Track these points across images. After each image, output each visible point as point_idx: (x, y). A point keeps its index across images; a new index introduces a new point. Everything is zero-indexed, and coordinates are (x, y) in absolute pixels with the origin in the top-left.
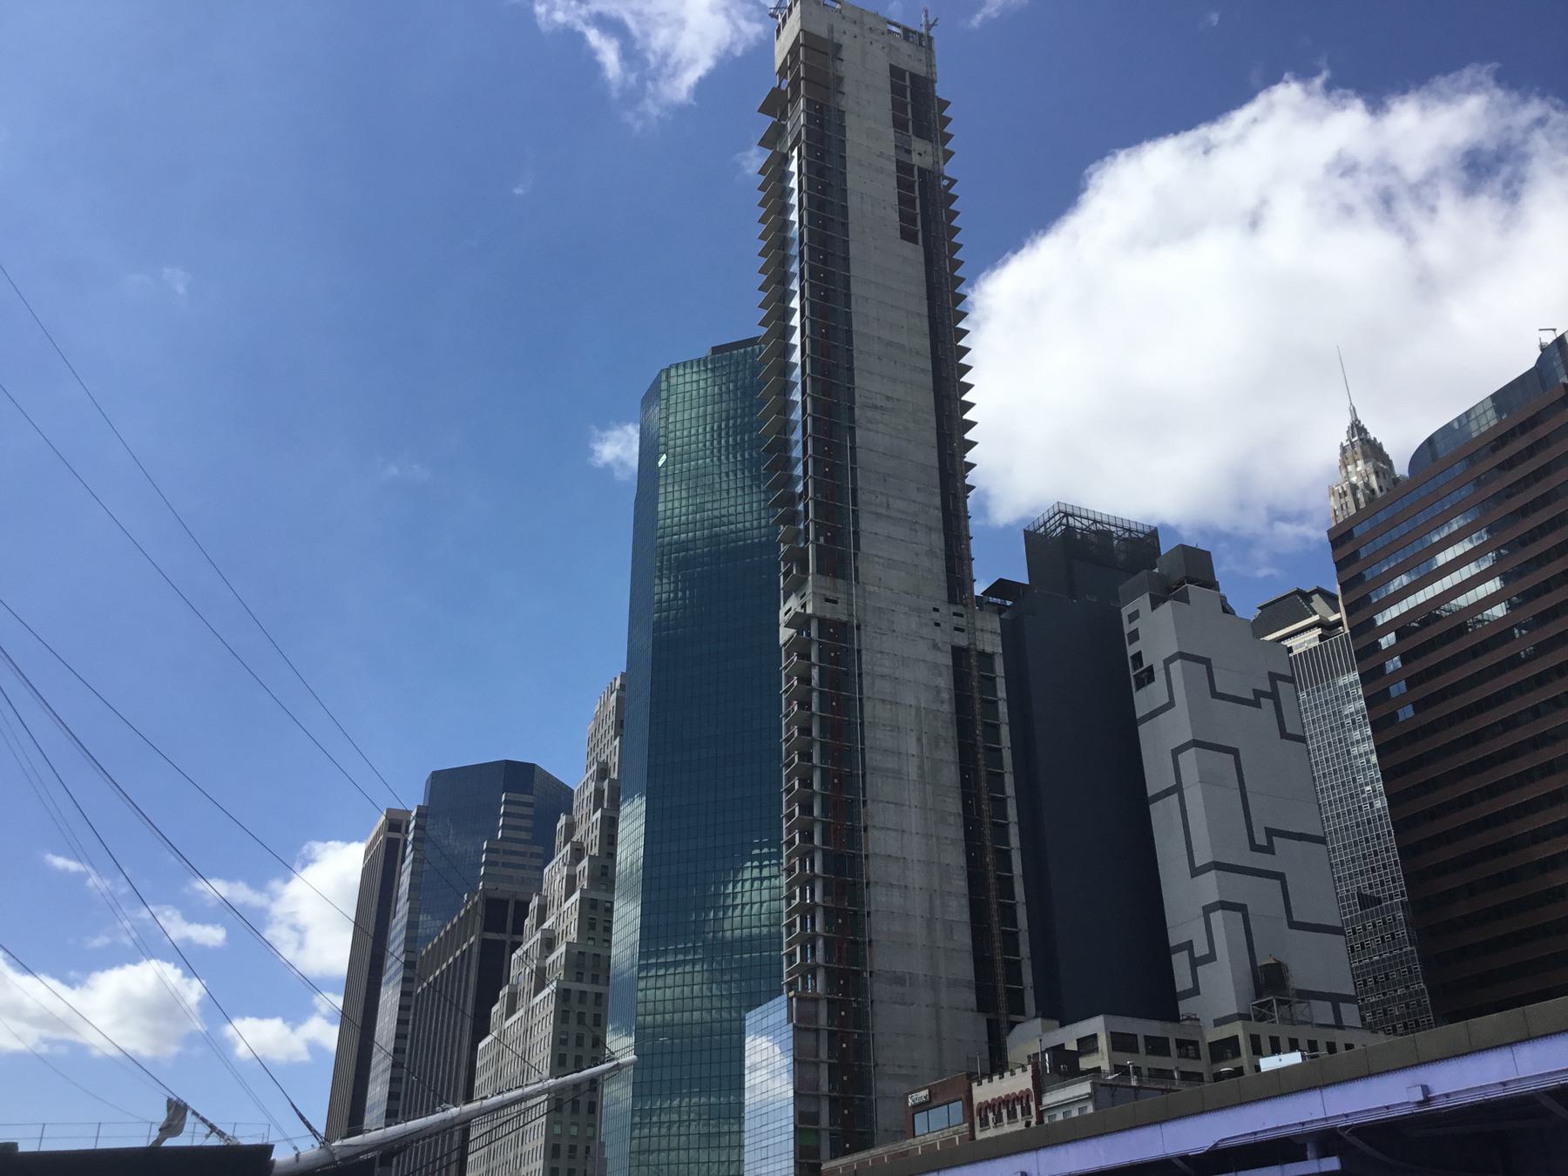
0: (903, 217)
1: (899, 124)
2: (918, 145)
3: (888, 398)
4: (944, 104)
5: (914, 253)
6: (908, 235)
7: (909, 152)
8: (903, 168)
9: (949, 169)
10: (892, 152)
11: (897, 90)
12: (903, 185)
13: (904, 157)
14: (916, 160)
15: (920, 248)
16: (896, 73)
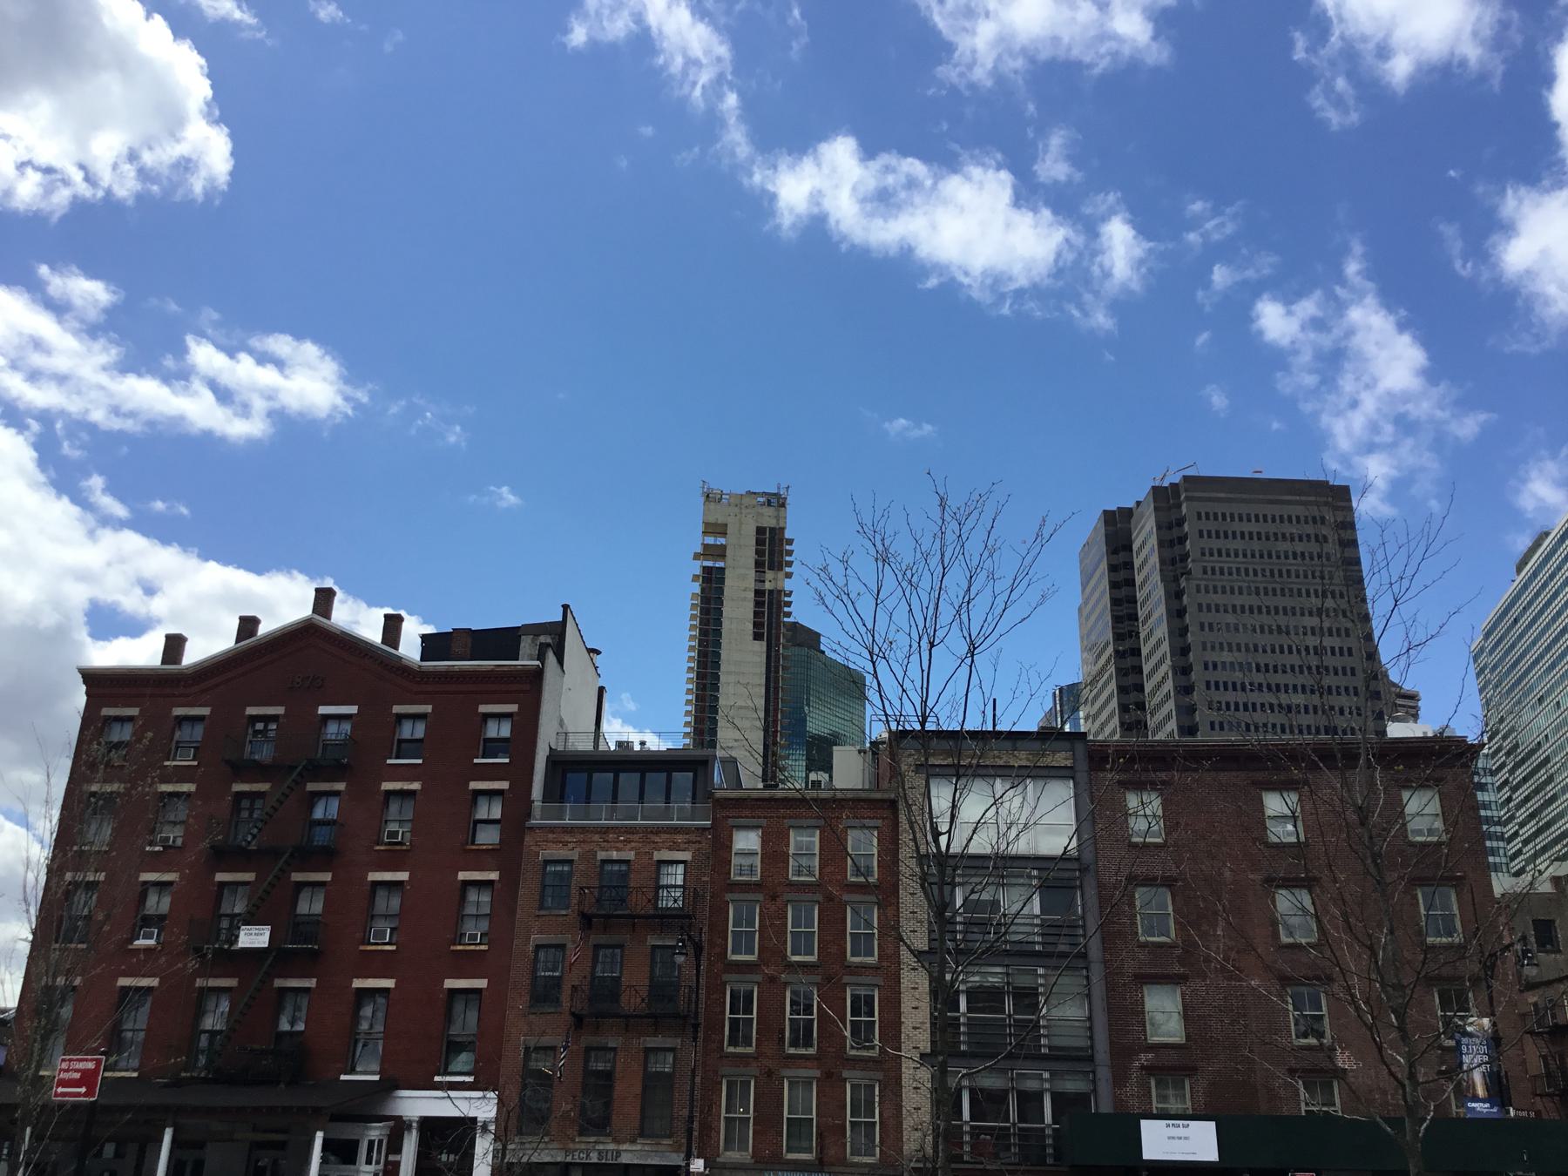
0: (755, 625)
1: (759, 565)
2: (769, 575)
3: (736, 740)
4: (790, 542)
5: (761, 646)
6: (757, 636)
7: (764, 581)
8: (759, 593)
9: (788, 585)
10: (751, 584)
11: (760, 542)
12: (758, 604)
13: (760, 586)
14: (768, 586)
15: (765, 643)
16: (760, 531)
